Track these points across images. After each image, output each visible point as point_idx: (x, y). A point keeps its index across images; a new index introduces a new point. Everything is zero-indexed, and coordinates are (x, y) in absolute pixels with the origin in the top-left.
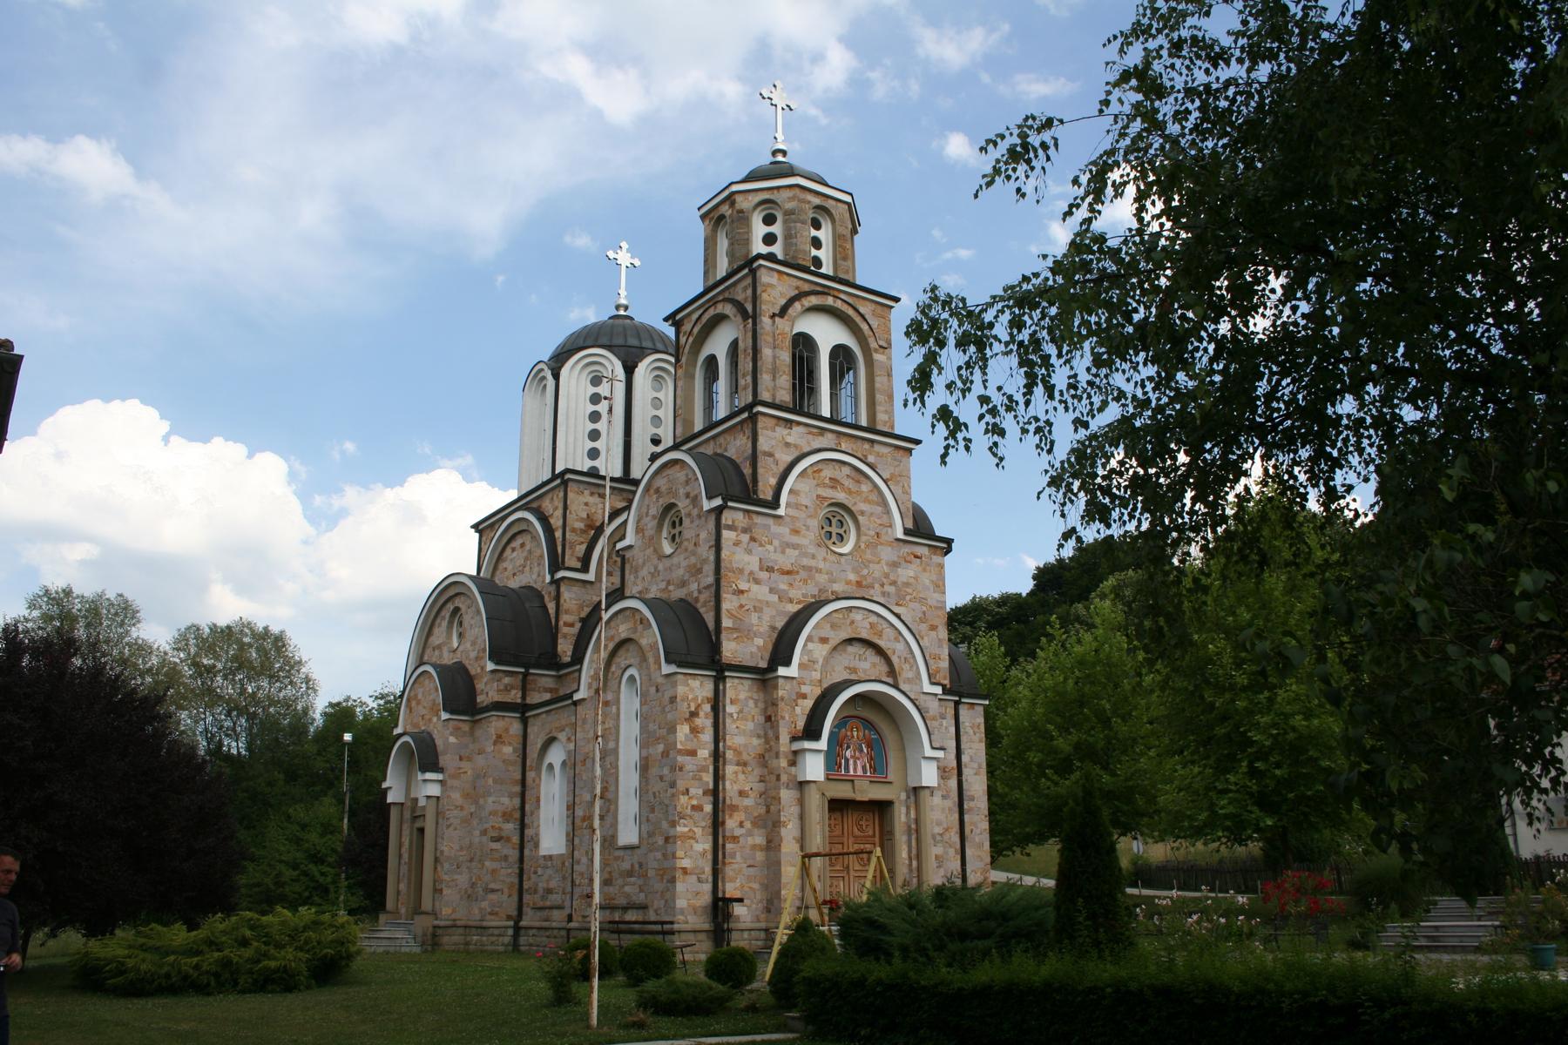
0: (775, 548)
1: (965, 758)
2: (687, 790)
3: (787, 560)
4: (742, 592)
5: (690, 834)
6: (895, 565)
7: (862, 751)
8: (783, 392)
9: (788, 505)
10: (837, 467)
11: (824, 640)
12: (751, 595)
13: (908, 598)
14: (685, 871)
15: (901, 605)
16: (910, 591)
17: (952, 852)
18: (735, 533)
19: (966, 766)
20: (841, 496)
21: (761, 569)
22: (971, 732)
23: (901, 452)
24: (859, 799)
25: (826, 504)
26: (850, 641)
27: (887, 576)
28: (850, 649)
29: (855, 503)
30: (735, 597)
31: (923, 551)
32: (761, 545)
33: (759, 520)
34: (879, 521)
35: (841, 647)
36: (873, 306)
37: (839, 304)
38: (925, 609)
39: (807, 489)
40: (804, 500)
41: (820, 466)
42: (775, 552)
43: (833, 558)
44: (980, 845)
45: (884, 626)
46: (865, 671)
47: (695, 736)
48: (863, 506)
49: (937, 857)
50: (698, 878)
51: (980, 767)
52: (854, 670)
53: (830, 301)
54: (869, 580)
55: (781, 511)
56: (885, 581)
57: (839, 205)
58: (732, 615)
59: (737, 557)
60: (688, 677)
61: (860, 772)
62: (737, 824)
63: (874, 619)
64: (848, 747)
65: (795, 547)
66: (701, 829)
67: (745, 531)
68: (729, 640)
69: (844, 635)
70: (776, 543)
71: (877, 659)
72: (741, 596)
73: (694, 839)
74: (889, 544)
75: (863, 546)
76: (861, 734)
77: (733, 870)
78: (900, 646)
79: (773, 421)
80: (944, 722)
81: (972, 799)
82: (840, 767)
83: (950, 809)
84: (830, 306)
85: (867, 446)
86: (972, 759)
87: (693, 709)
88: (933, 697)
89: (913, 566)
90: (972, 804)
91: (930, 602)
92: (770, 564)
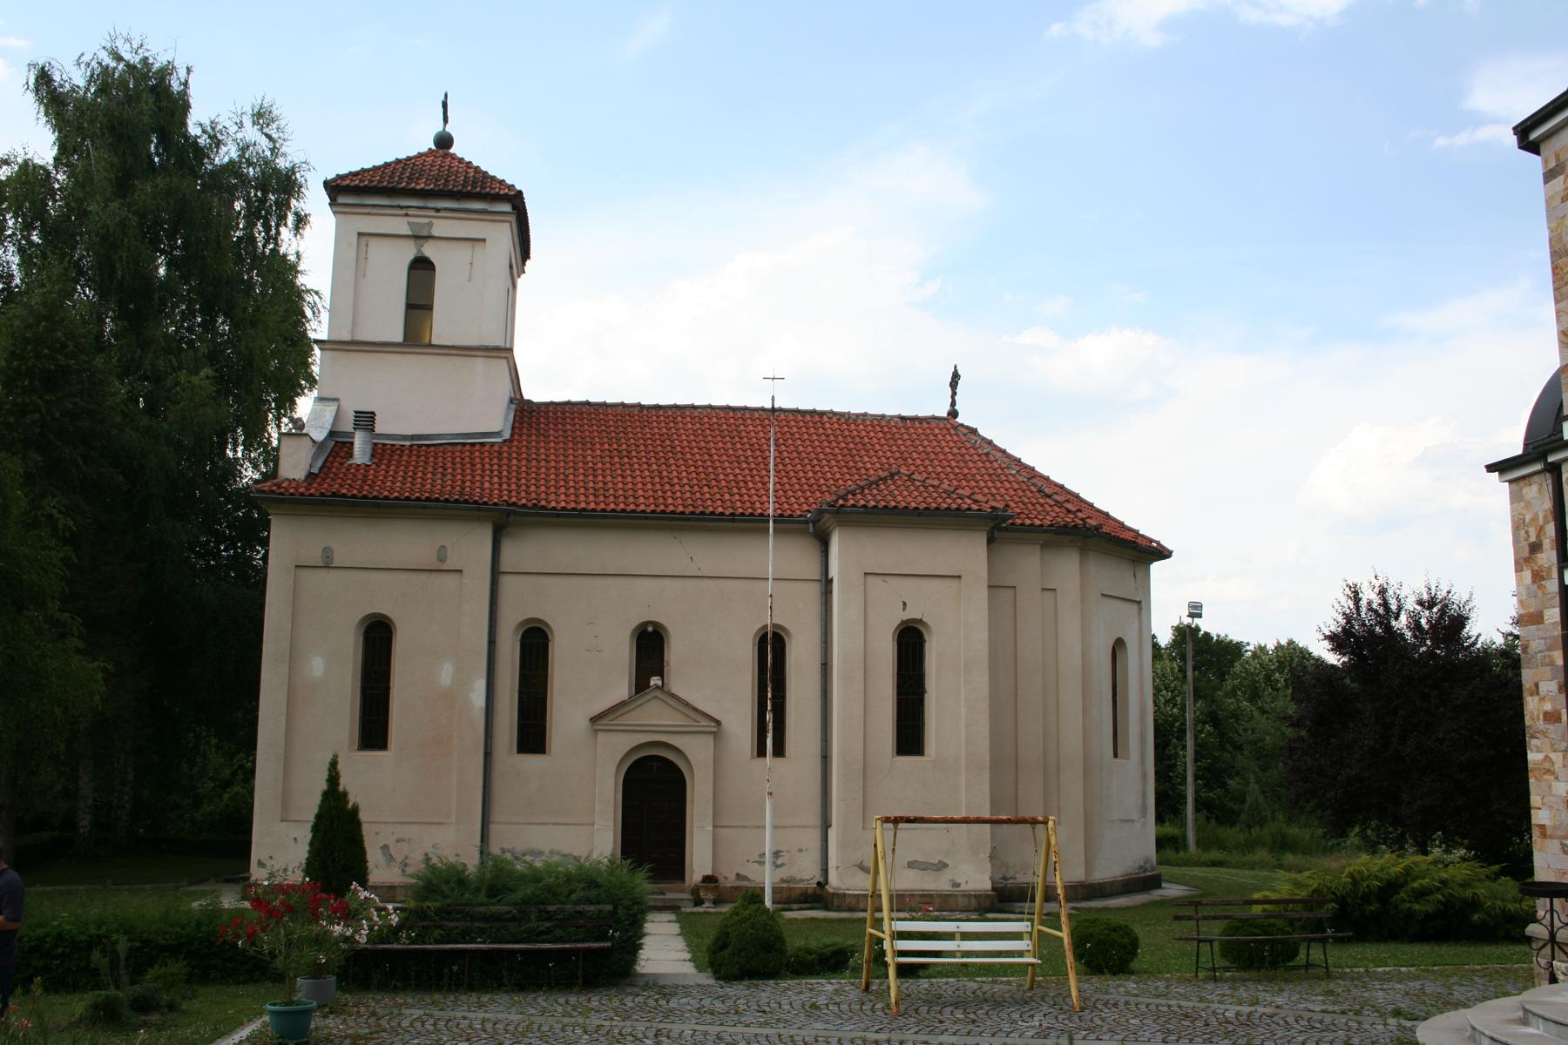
2: (1537, 685)
5: (1547, 765)
14: (1542, 827)
47: (1541, 587)
50: (1562, 844)
60: (1522, 483)
66: (1561, 754)
73: (1549, 771)
87: (1533, 539)
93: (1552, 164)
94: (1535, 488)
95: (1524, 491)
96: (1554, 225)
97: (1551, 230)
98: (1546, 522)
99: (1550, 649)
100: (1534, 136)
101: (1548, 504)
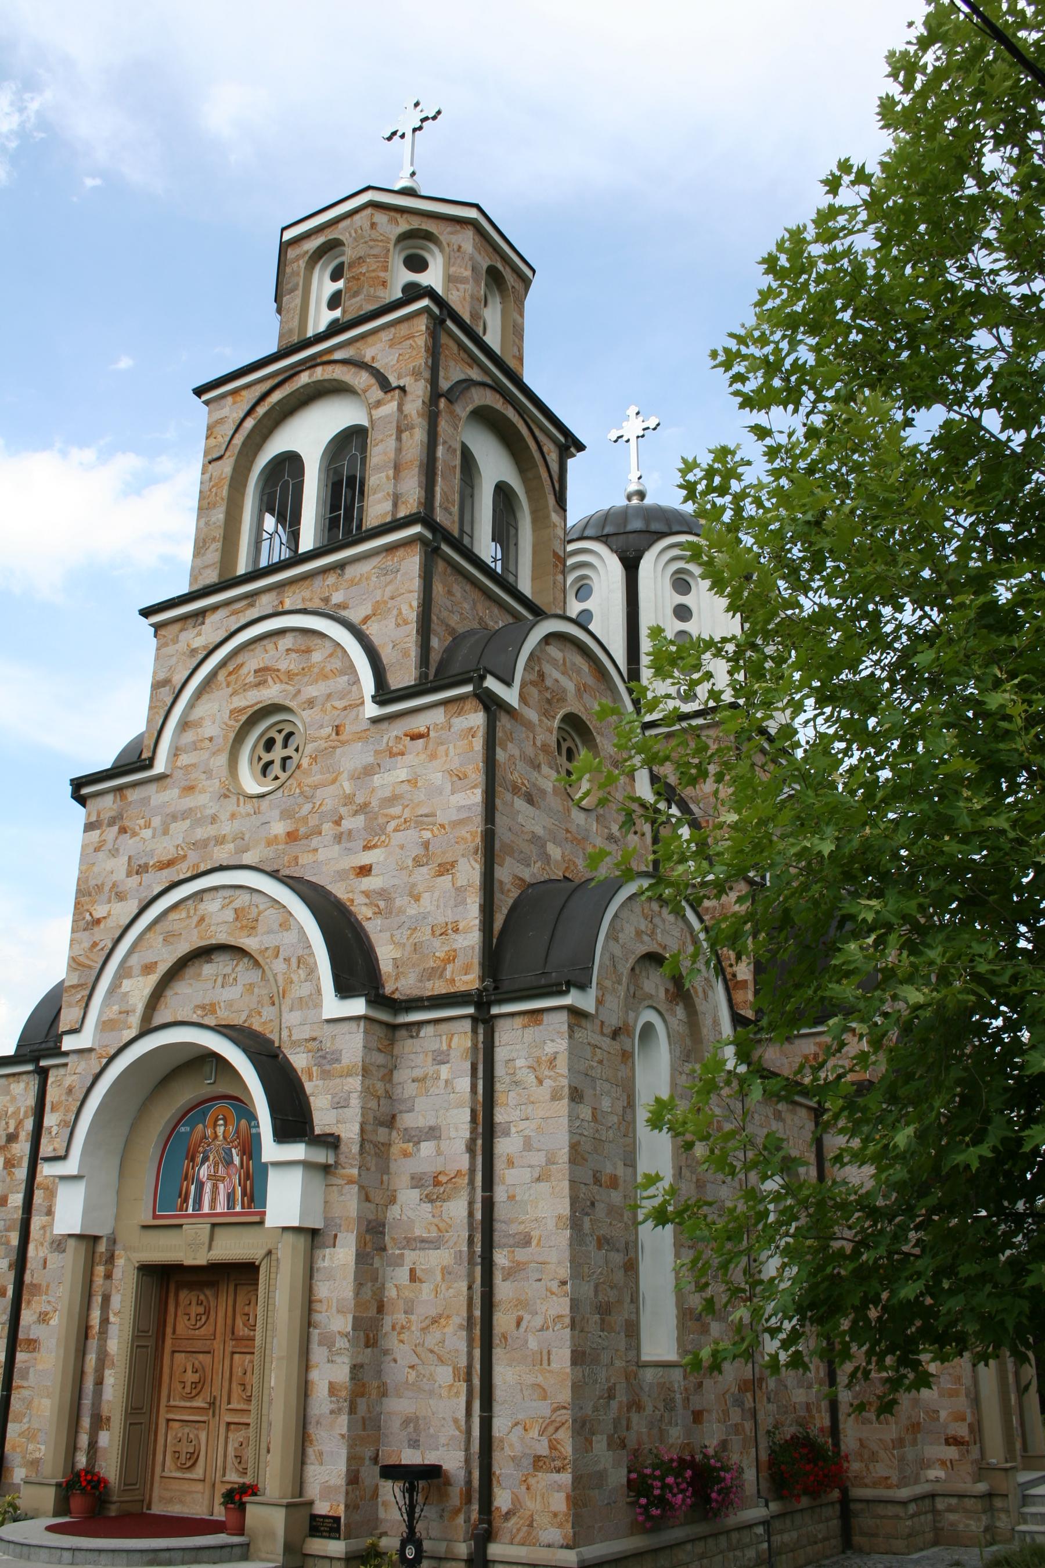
0: (155, 829)
1: (503, 1147)
3: (165, 848)
4: (98, 922)
6: (368, 771)
7: (229, 1163)
8: (209, 571)
9: (176, 752)
10: (268, 644)
11: (148, 969)
12: (109, 920)
13: (392, 825)
15: (375, 846)
16: (396, 810)
17: (444, 1375)
18: (98, 832)
19: (510, 1163)
20: (272, 693)
21: (129, 874)
22: (532, 1078)
23: (401, 553)
24: (188, 1262)
25: (244, 718)
26: (205, 953)
27: (348, 800)
28: (208, 969)
29: (299, 691)
30: (87, 933)
31: (438, 716)
32: (134, 834)
33: (133, 795)
34: (340, 704)
35: (190, 971)
36: (385, 336)
37: (320, 373)
38: (427, 835)
39: (216, 707)
40: (210, 729)
41: (239, 659)
42: (153, 837)
43: (248, 807)
44: (544, 1358)
45: (262, 907)
46: (230, 1004)
47: (10, 1174)
48: (312, 691)
49: (333, 1389)
51: (550, 1161)
52: (210, 1008)
53: (304, 378)
54: (313, 821)
55: (160, 766)
56: (343, 810)
57: (357, 217)
58: (79, 964)
59: (96, 869)
60: (11, 1079)
61: (221, 1207)
62: (35, 1317)
63: (244, 898)
64: (206, 1159)
65: (186, 814)
67: (112, 822)
68: (70, 1006)
69: (183, 948)
70: (156, 821)
71: (254, 976)
72: (96, 929)
74: (361, 737)
75: (305, 762)
76: (231, 1129)
77: (23, 1400)
78: (288, 938)
79: (177, 627)
80: (445, 1071)
81: (526, 1241)
82: (186, 1200)
83: (446, 1271)
84: (308, 384)
85: (331, 579)
86: (528, 1145)
87: (11, 1130)
88: (353, 1025)
89: (409, 759)
90: (521, 1254)
91: (440, 819)
92: (142, 862)
93: (93, 819)
94: (22, 1085)
95: (12, 1086)
96: (84, 868)
97: (81, 872)
98: (26, 1117)
99: (7, 1230)
100: (85, 791)
101: (31, 1101)
